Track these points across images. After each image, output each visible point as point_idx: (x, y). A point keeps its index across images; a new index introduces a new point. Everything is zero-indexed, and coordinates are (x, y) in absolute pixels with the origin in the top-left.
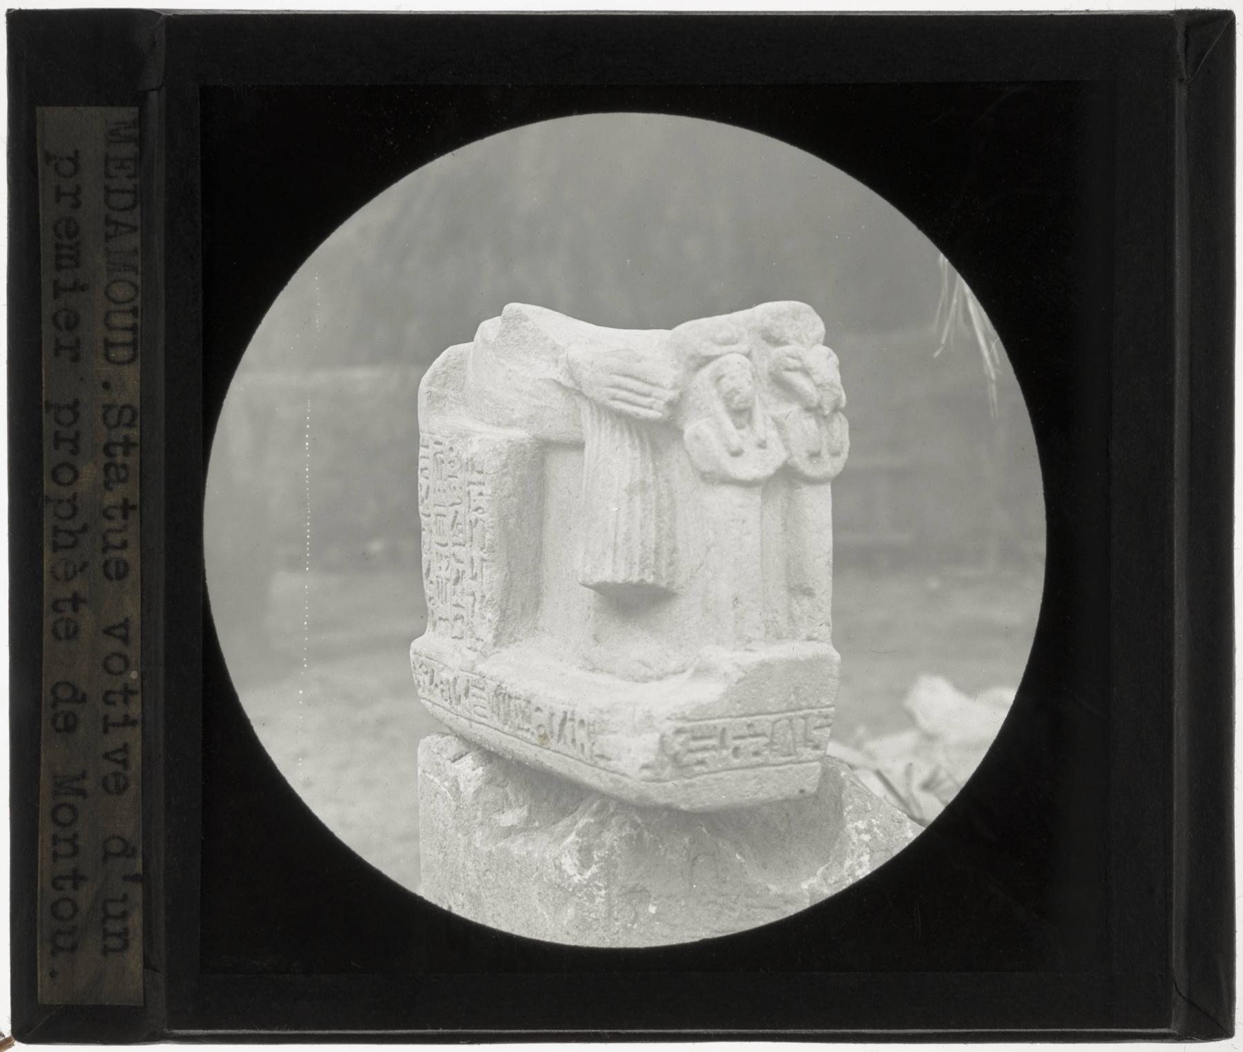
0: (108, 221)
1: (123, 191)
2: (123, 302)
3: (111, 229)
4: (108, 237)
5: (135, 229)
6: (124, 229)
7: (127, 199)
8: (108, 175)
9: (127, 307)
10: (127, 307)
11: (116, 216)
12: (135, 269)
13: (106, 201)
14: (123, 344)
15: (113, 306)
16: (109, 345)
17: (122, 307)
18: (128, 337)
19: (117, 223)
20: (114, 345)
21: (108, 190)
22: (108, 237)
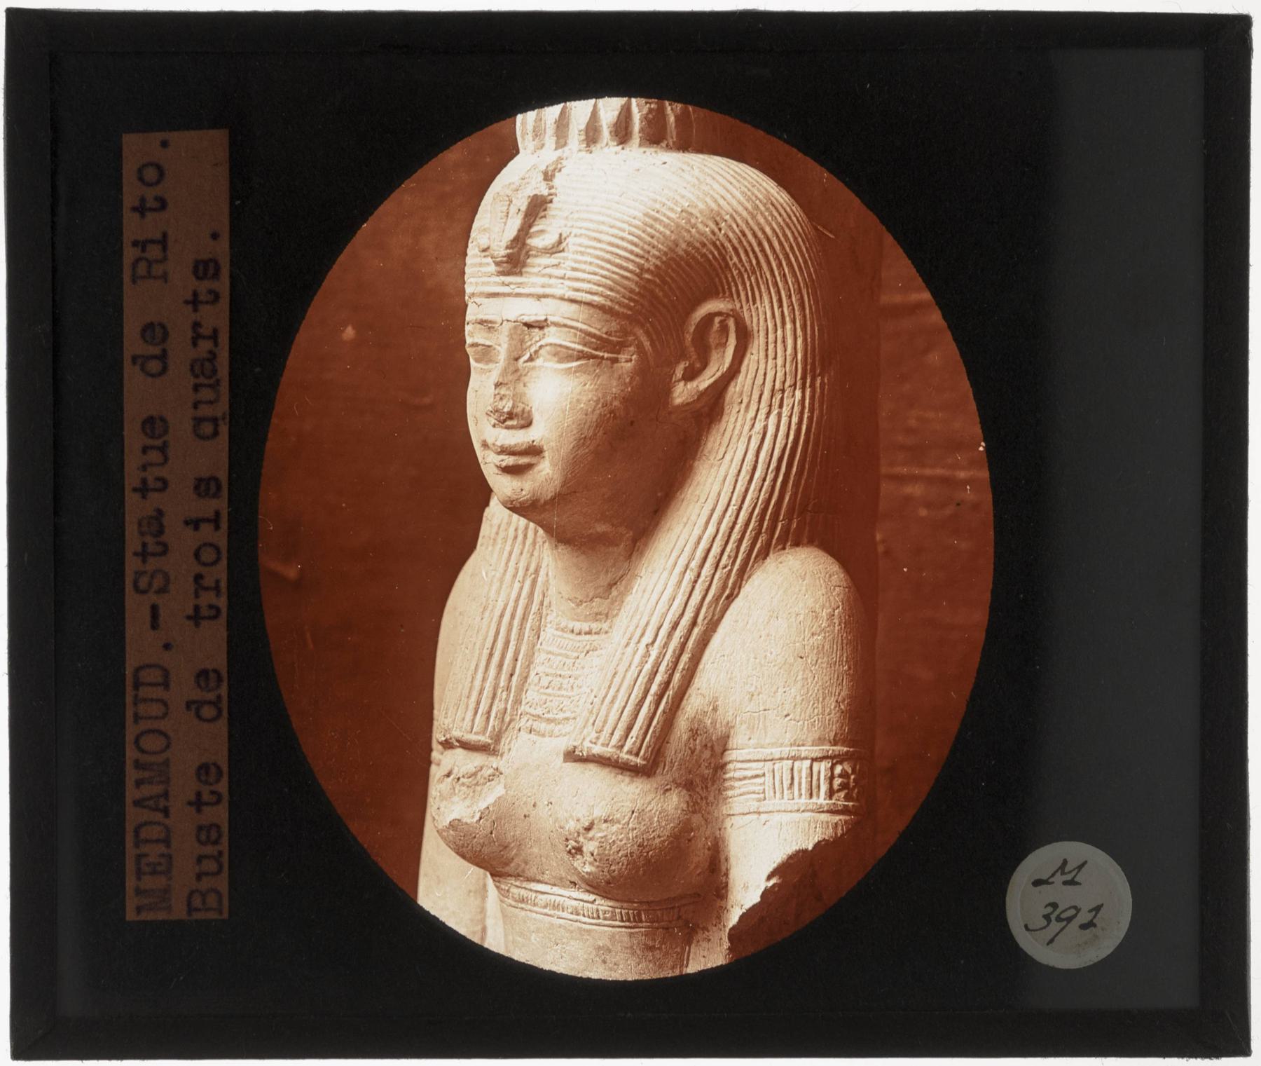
0: (166, 812)
1: (147, 841)
3: (162, 803)
5: (137, 803)
8: (170, 857)
11: (159, 816)
13: (168, 829)
19: (156, 809)
21: (167, 842)
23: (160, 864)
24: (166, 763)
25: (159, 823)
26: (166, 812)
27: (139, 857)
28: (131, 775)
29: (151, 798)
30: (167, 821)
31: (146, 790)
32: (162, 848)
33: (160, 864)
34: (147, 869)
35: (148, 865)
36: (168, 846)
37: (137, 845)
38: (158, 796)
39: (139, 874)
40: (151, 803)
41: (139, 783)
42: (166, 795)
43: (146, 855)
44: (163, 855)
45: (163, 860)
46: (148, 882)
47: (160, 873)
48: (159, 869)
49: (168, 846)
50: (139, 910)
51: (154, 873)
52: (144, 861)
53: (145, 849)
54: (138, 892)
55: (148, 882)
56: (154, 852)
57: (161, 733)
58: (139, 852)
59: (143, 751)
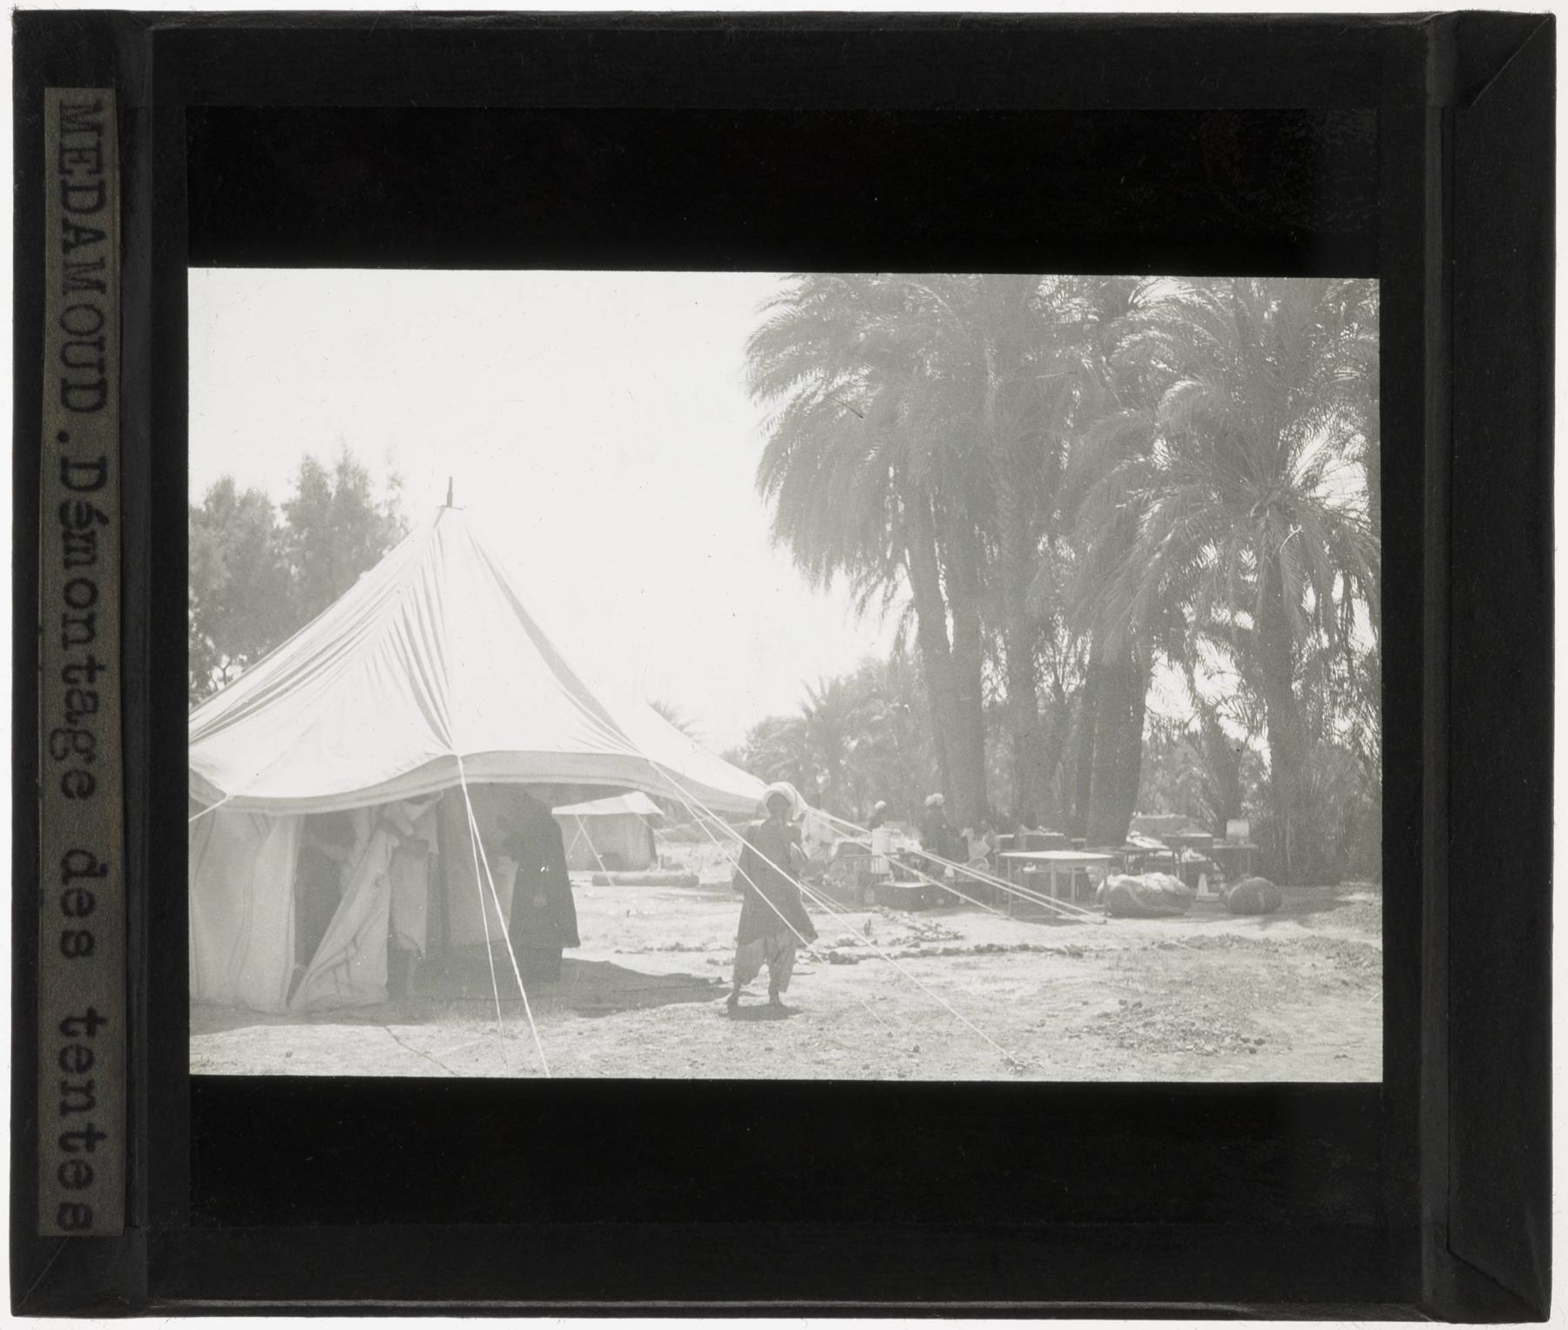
0: (66, 226)
1: (88, 189)
2: (89, 333)
4: (67, 247)
6: (85, 236)
7: (90, 199)
9: (94, 338)
11: (75, 219)
12: (100, 286)
13: (66, 205)
14: (84, 387)
15: (74, 338)
16: (66, 387)
17: (85, 338)
18: (92, 376)
19: (79, 230)
21: (66, 188)
22: (67, 247)
25: (76, 211)
26: (66, 226)
27: (99, 169)
28: (109, 275)
31: (88, 253)
32: (72, 181)
33: (72, 161)
34: (87, 155)
35: (87, 161)
36: (64, 183)
37: (101, 187)
38: (73, 246)
39: (98, 149)
40: (85, 236)
41: (101, 264)
43: (90, 172)
44: (70, 172)
45: (68, 166)
49: (64, 183)
50: (97, 108)
51: (81, 151)
52: (92, 166)
53: (92, 181)
54: (97, 128)
55: (89, 140)
56: (80, 175)
57: (70, 332)
58: (97, 177)
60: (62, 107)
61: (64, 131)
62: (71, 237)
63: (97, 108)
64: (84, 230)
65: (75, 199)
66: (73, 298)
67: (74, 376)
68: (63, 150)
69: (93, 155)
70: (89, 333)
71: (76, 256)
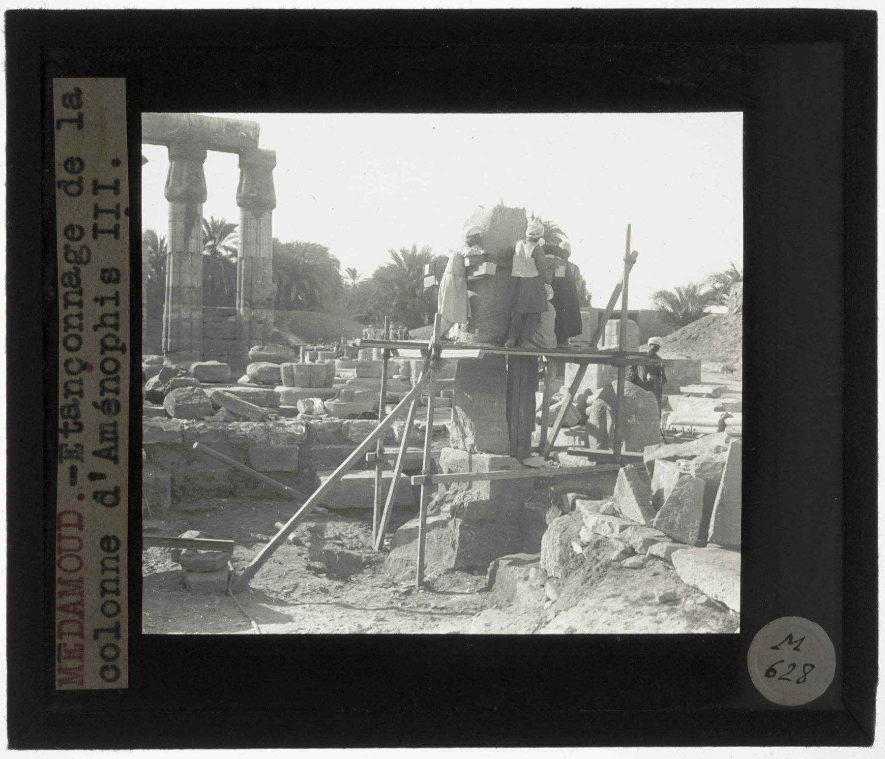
0: (81, 614)
1: (69, 634)
9: (64, 554)
10: (64, 554)
11: (76, 617)
13: (82, 627)
14: (68, 525)
16: (80, 526)
18: (65, 531)
19: (74, 612)
20: (74, 525)
21: (81, 634)
23: (75, 651)
24: (81, 580)
29: (70, 605)
30: (81, 620)
32: (77, 640)
33: (75, 651)
40: (71, 608)
41: (61, 595)
42: (81, 603)
43: (65, 645)
46: (69, 664)
47: (75, 658)
48: (76, 654)
50: (61, 682)
52: (63, 649)
54: (61, 670)
55: (69, 664)
56: (70, 642)
57: (77, 557)
59: (65, 570)
60: (82, 682)
61: (81, 668)
62: (79, 607)
63: (61, 682)
64: (68, 611)
65: (75, 628)
66: (75, 576)
67: (74, 531)
68: (81, 658)
69: (63, 653)
70: (65, 557)
71: (74, 599)
